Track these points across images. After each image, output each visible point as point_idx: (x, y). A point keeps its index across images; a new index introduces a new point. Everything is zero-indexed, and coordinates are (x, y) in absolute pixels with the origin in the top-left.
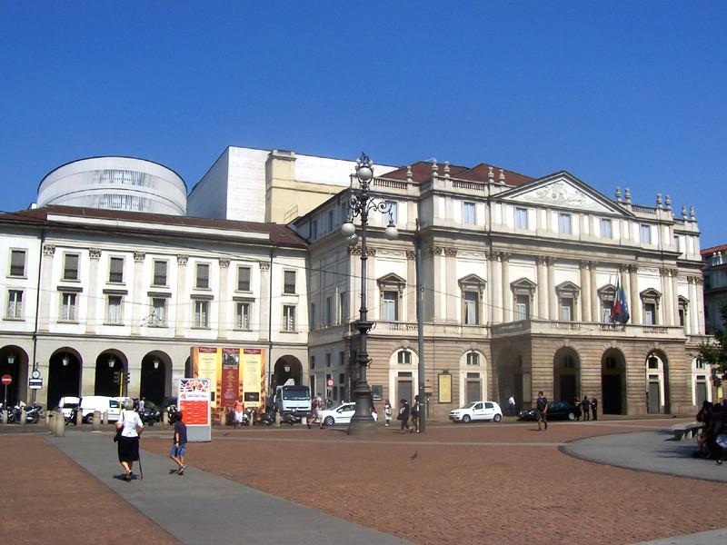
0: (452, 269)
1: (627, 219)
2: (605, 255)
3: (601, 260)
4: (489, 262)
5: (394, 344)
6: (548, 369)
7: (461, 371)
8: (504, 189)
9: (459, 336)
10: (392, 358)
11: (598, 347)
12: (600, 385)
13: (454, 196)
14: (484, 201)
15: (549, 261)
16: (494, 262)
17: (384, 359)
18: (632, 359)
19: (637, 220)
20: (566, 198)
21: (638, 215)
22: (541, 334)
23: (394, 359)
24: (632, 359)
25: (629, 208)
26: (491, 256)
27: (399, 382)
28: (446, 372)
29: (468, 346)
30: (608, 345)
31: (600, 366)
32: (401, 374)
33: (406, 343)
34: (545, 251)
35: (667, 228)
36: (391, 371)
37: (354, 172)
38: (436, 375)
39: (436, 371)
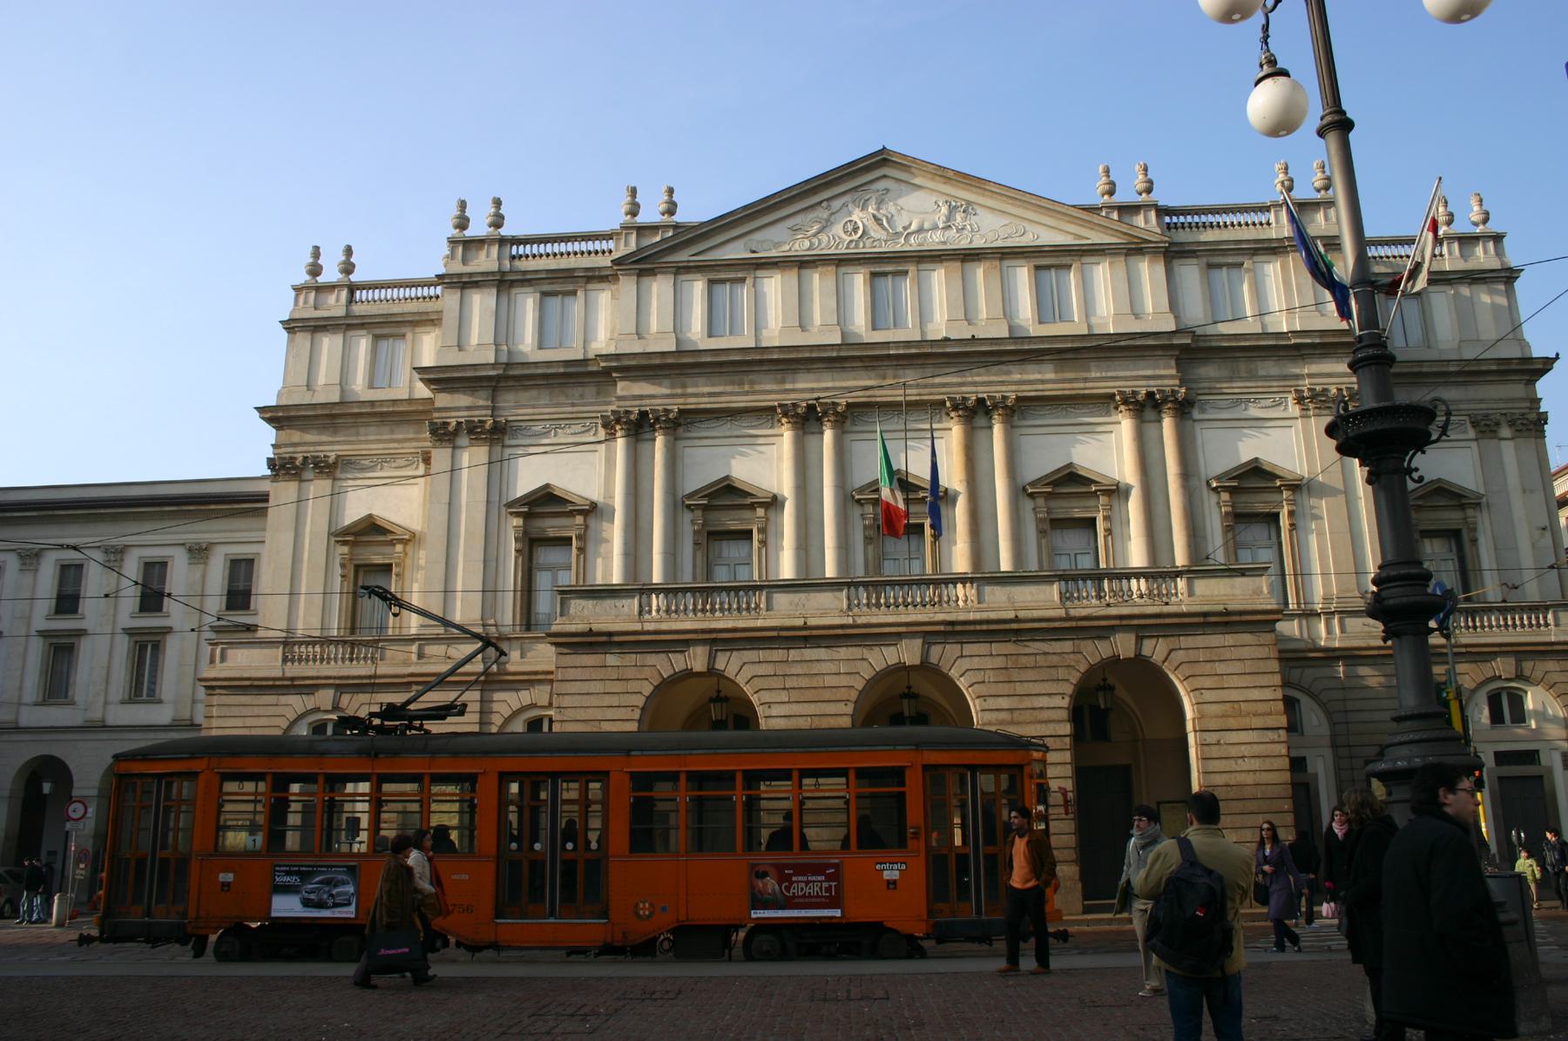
3: (1029, 391)
18: (1004, 703)
22: (591, 633)
24: (1004, 703)
34: (806, 387)
37: (303, 278)
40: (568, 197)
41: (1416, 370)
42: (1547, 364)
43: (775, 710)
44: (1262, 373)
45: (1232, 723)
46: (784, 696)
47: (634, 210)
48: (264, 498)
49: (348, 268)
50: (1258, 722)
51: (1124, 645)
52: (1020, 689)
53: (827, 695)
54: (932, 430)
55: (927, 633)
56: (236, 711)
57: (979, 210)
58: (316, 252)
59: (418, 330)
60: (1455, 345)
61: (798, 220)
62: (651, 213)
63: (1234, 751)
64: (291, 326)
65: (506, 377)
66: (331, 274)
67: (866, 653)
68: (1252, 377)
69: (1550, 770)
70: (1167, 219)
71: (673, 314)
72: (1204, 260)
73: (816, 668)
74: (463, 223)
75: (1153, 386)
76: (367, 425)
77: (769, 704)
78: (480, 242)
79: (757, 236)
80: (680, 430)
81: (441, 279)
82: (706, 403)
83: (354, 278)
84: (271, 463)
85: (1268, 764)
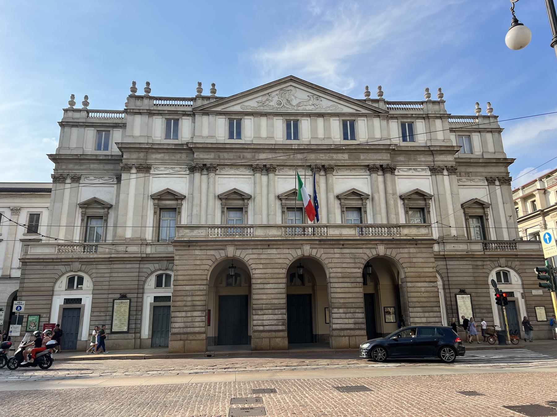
0: (146, 185)
1: (379, 116)
2: (346, 156)
4: (192, 175)
5: (62, 268)
6: (202, 287)
7: (145, 296)
8: (215, 100)
9: (145, 256)
10: (59, 282)
11: (282, 256)
12: (285, 306)
13: (151, 113)
14: (188, 115)
15: (267, 169)
16: (197, 175)
17: (48, 284)
19: (393, 117)
20: (294, 103)
21: (392, 112)
23: (63, 282)
24: (339, 270)
25: (381, 105)
26: (192, 169)
27: (64, 309)
28: (123, 297)
29: (157, 266)
30: (297, 254)
31: (285, 281)
32: (67, 301)
33: (77, 265)
35: (438, 122)
36: (55, 298)
37: (68, 106)
38: (111, 300)
39: (110, 296)
40: (175, 85)
41: (469, 161)
42: (512, 161)
43: (257, 271)
44: (419, 160)
45: (418, 279)
46: (261, 266)
47: (200, 90)
48: (49, 190)
49: (86, 103)
50: (427, 279)
51: (381, 250)
52: (344, 265)
53: (276, 266)
54: (305, 175)
55: (311, 244)
56: (37, 272)
57: (322, 99)
58: (73, 96)
59: (114, 129)
60: (481, 153)
61: (260, 99)
62: (206, 92)
63: (419, 289)
64: (62, 124)
65: (151, 149)
66: (79, 105)
67: (290, 251)
68: (416, 160)
69: (517, 299)
70: (387, 106)
71: (215, 129)
72: (399, 121)
73: (272, 256)
74: (134, 89)
75: (381, 162)
76: (94, 163)
77: (255, 269)
78: (141, 98)
79: (246, 104)
80: (217, 172)
81: (125, 111)
82: (227, 162)
83: (89, 108)
84: (54, 177)
85: (431, 295)
